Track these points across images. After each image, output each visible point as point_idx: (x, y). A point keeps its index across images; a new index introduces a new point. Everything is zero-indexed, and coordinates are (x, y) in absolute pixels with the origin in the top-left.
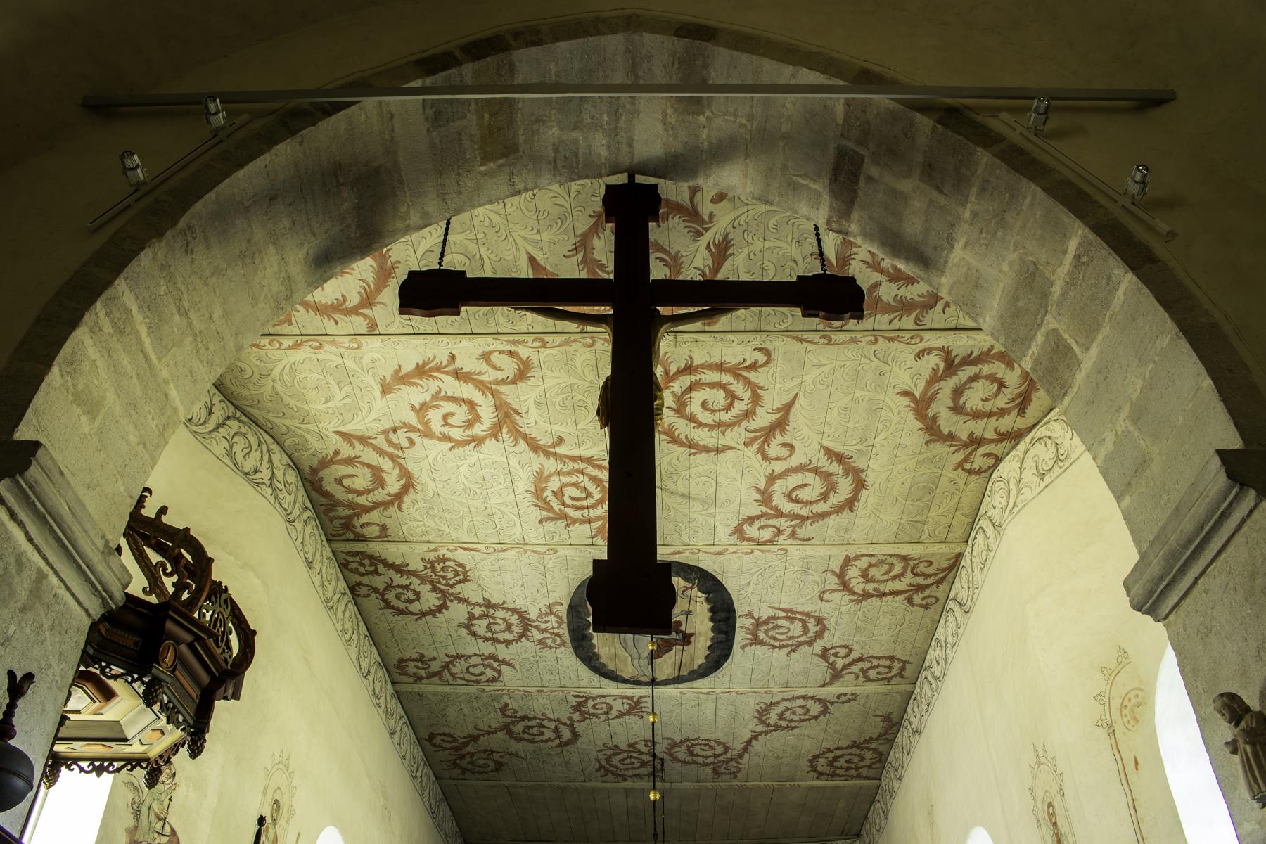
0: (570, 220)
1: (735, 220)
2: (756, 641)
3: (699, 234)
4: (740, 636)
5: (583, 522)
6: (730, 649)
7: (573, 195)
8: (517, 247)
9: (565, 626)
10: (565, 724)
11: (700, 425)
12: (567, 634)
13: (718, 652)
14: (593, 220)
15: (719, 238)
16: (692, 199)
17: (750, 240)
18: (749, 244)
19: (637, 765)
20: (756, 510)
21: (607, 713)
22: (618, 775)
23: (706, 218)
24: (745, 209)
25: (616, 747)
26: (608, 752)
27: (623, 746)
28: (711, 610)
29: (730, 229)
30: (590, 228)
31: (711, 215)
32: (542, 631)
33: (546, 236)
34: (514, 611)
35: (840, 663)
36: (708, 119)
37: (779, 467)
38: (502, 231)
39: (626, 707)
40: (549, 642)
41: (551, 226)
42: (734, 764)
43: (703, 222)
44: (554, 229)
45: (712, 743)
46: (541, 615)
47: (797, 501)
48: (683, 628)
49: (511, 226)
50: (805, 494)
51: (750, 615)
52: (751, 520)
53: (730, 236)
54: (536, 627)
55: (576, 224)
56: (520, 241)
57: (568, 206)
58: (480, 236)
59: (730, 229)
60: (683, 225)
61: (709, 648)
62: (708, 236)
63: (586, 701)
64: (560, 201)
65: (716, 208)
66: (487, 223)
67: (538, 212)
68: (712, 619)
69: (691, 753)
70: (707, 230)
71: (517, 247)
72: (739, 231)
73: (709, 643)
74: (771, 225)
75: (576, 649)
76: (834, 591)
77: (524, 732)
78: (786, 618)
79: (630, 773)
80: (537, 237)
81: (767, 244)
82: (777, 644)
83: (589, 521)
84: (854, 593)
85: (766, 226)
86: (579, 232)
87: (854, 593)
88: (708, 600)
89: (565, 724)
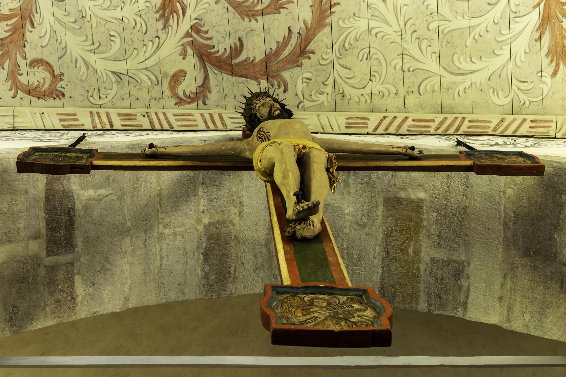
0: (336, 47)
1: (158, 48)
3: (196, 28)
7: (331, 80)
8: (395, 9)
14: (311, 47)
15: (173, 22)
16: (206, 76)
17: (138, 19)
18: (139, 13)
23: (190, 51)
24: (149, 63)
30: (314, 35)
31: (184, 54)
33: (362, 25)
36: (199, 221)
38: (409, 33)
41: (356, 40)
43: (193, 44)
44: (353, 35)
49: (398, 40)
53: (161, 24)
55: (329, 42)
56: (391, 17)
57: (337, 66)
58: (433, 26)
59: (163, 36)
60: (214, 42)
62: (185, 26)
64: (344, 73)
66: (425, 43)
67: (369, 58)
70: (188, 35)
71: (395, 9)
72: (152, 33)
74: (117, 40)
80: (373, 24)
81: (117, 14)
85: (124, 42)
86: (327, 30)
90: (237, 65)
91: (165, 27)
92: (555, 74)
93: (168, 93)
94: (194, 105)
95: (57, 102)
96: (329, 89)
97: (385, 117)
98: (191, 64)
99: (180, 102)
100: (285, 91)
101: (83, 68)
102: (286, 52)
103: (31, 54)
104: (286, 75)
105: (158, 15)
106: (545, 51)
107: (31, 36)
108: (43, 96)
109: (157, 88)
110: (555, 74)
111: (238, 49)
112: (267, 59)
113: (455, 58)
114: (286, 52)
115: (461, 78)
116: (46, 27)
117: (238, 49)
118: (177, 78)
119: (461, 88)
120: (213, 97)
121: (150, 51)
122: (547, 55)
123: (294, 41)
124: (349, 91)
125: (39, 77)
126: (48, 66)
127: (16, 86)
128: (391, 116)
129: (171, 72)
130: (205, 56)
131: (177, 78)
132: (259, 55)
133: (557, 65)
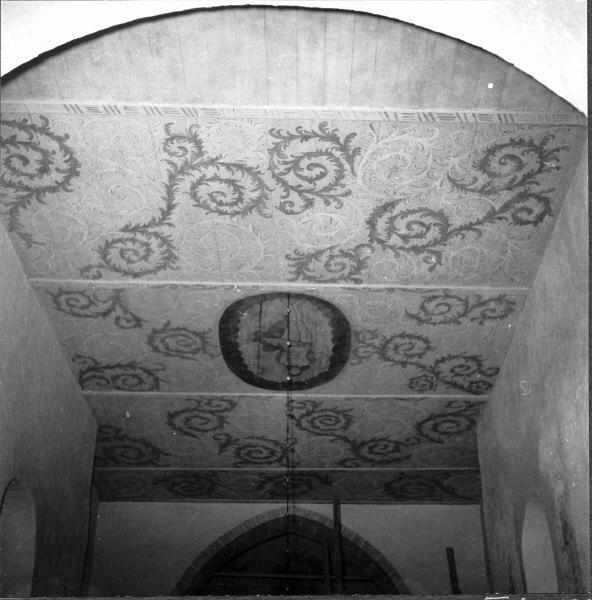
2: (201, 335)
4: (215, 338)
5: (327, 410)
6: (221, 329)
9: (353, 348)
10: (380, 242)
11: (263, 447)
12: (353, 342)
13: (231, 325)
19: (304, 163)
20: (225, 414)
21: (331, 257)
22: (334, 138)
25: (327, 203)
26: (339, 191)
27: (319, 202)
28: (242, 359)
32: (372, 345)
34: (389, 360)
35: (119, 312)
37: (218, 431)
39: (311, 266)
40: (369, 336)
42: (179, 162)
45: (213, 205)
46: (368, 358)
47: (205, 418)
48: (262, 346)
50: (200, 421)
51: (212, 356)
52: (227, 410)
54: (375, 347)
61: (238, 330)
63: (350, 274)
68: (240, 353)
69: (237, 188)
73: (239, 333)
75: (349, 330)
76: (157, 370)
77: (428, 228)
78: (182, 352)
79: (312, 145)
82: (183, 332)
83: (323, 410)
84: (141, 368)
87: (141, 368)
88: (246, 366)
89: (380, 242)
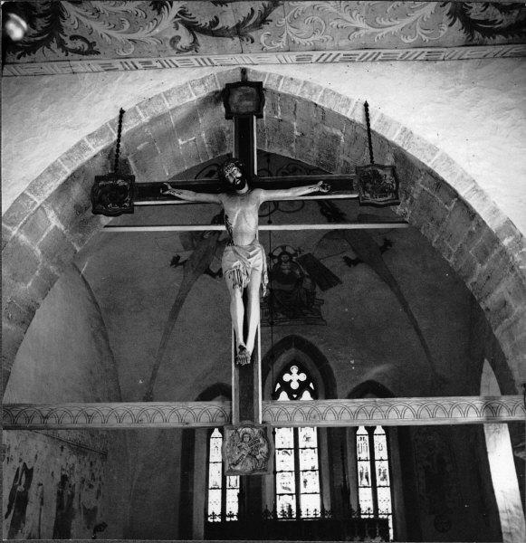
16: (195, 38)
17: (139, 11)
23: (180, 25)
29: (159, 18)
30: (270, 11)
43: (183, 22)
64: (294, 31)
65: (175, 33)
70: (177, 17)
74: (127, 22)
90: (217, 30)
91: (159, 13)
92: (451, 25)
93: (170, 48)
94: (190, 52)
95: (95, 56)
96: (284, 39)
97: (323, 55)
98: (183, 31)
99: (179, 52)
100: (253, 42)
101: (108, 38)
102: (251, 22)
103: (70, 34)
104: (253, 34)
105: (152, 7)
106: (447, 11)
107: (66, 24)
108: (86, 53)
109: (163, 46)
110: (451, 25)
111: (215, 22)
112: (238, 26)
113: (377, 20)
114: (251, 22)
115: (379, 30)
116: (73, 18)
117: (215, 22)
118: (174, 40)
119: (380, 35)
120: (202, 48)
121: (152, 27)
122: (448, 15)
123: (256, 16)
124: (297, 40)
125: (79, 44)
126: (84, 39)
127: (66, 51)
128: (328, 53)
129: (170, 37)
130: (192, 28)
131: (174, 40)
132: (231, 25)
133: (454, 21)
